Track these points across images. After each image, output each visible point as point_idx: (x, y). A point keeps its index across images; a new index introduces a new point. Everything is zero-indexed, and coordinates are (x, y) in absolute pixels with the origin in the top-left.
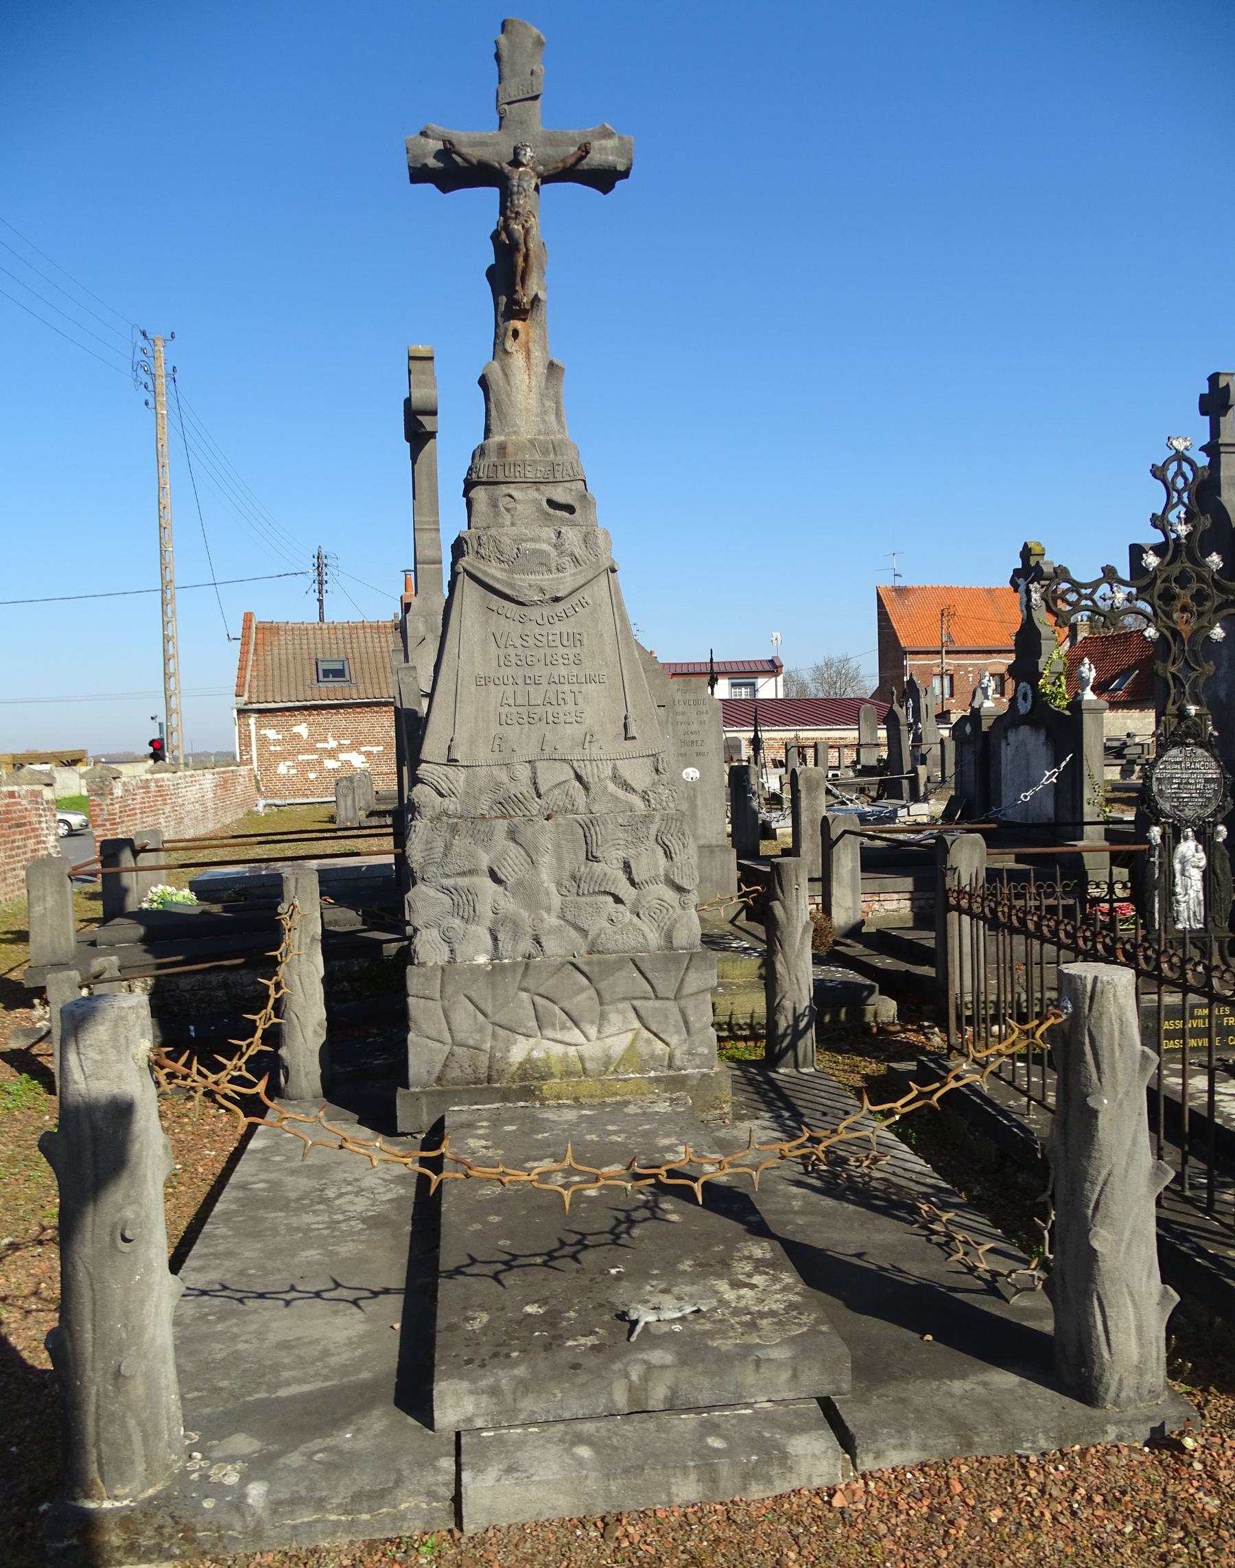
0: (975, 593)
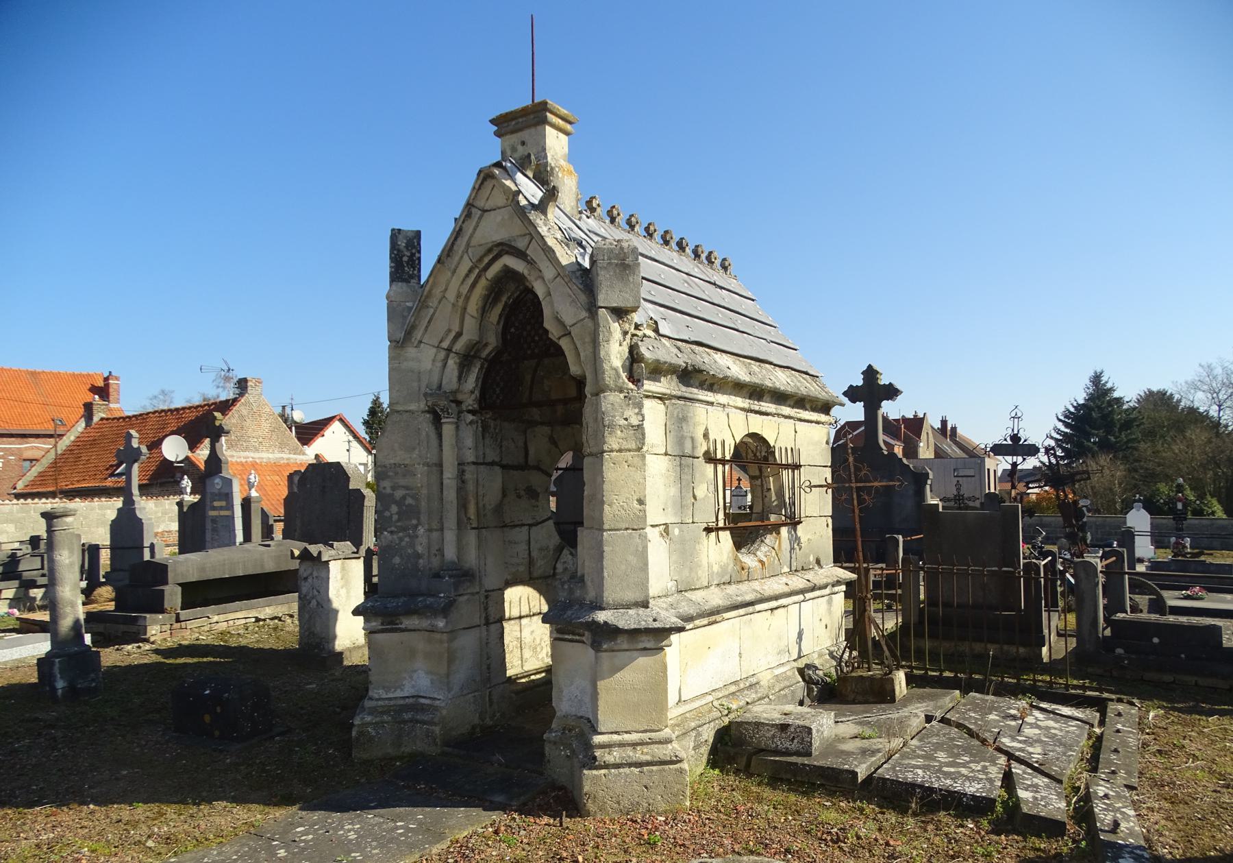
0: (16, 375)
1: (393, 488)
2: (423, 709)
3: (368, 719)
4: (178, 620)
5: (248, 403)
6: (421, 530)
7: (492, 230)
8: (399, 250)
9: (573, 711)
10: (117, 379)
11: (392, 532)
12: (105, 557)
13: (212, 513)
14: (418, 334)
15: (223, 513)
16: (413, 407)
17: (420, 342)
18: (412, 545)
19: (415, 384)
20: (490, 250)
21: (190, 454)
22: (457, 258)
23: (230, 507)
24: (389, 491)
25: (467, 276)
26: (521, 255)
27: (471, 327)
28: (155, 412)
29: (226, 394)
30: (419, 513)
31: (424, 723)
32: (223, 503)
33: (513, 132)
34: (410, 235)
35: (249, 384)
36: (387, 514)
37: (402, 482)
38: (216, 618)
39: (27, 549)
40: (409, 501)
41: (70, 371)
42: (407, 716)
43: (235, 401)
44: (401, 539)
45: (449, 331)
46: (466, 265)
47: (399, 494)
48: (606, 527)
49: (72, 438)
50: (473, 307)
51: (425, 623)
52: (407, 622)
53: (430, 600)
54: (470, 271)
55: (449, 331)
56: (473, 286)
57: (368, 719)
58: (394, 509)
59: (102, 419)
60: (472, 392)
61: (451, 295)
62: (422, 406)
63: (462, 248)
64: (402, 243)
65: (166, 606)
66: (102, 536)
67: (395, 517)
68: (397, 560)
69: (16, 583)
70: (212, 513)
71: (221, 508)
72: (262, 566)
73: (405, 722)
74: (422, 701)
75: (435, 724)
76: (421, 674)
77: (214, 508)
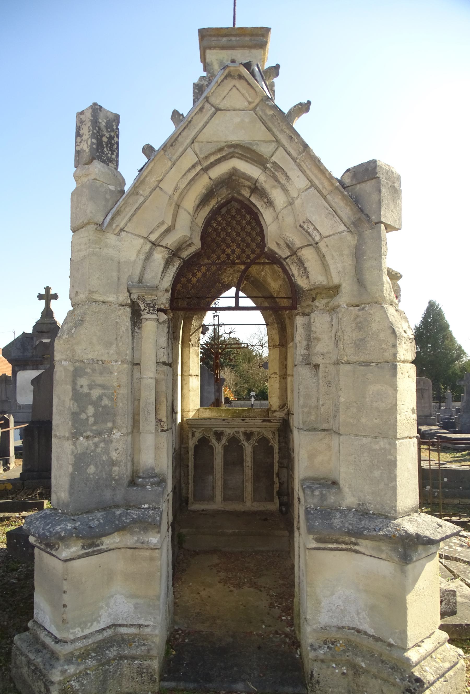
1: (91, 387)
2: (122, 641)
3: (71, 669)
6: (117, 434)
7: (231, 127)
8: (99, 128)
9: (335, 622)
11: (87, 437)
14: (121, 222)
16: (111, 298)
17: (122, 230)
18: (106, 451)
19: (115, 274)
20: (221, 150)
22: (181, 150)
24: (85, 390)
25: (189, 170)
26: (259, 160)
27: (184, 220)
30: (115, 415)
31: (133, 658)
33: (223, 48)
34: (111, 117)
36: (83, 416)
37: (99, 380)
40: (106, 402)
42: (112, 653)
44: (96, 445)
45: (163, 223)
46: (189, 159)
47: (96, 393)
48: (398, 436)
50: (190, 202)
51: (130, 540)
52: (113, 540)
53: (134, 513)
54: (193, 166)
55: (163, 223)
56: (190, 183)
57: (71, 669)
58: (91, 410)
60: (167, 291)
61: (168, 187)
62: (123, 297)
63: (189, 140)
64: (103, 123)
67: (92, 420)
68: (92, 469)
73: (108, 662)
74: (123, 630)
75: (151, 658)
76: (120, 598)
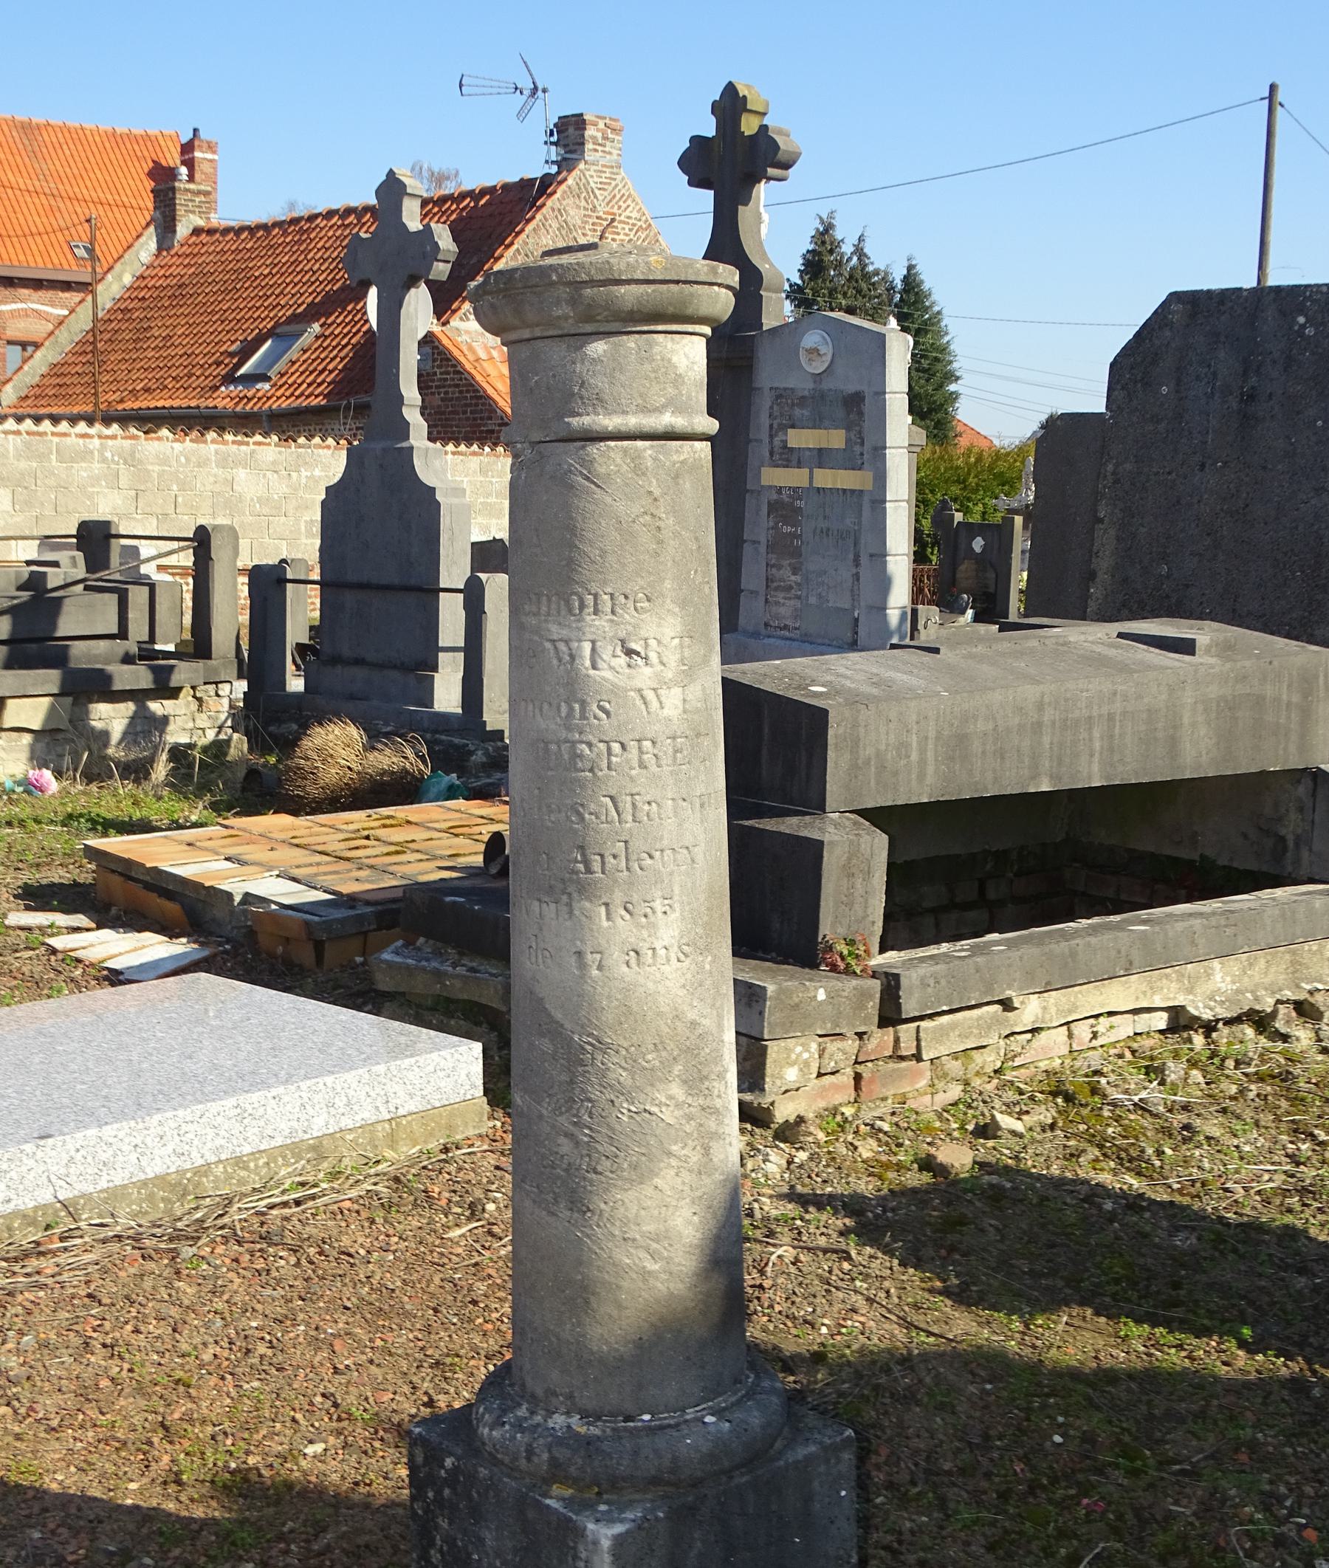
4: (890, 1015)
5: (584, 192)
10: (211, 147)
12: (303, 611)
13: (775, 477)
15: (826, 478)
21: (437, 329)
23: (867, 452)
28: (330, 214)
29: (532, 160)
32: (835, 439)
35: (590, 132)
38: (1030, 1010)
39: (71, 566)
41: (105, 126)
43: (545, 185)
49: (128, 279)
59: (197, 231)
65: (828, 928)
66: (298, 541)
69: (50, 679)
70: (775, 477)
71: (822, 458)
72: (1173, 744)
77: (789, 457)
